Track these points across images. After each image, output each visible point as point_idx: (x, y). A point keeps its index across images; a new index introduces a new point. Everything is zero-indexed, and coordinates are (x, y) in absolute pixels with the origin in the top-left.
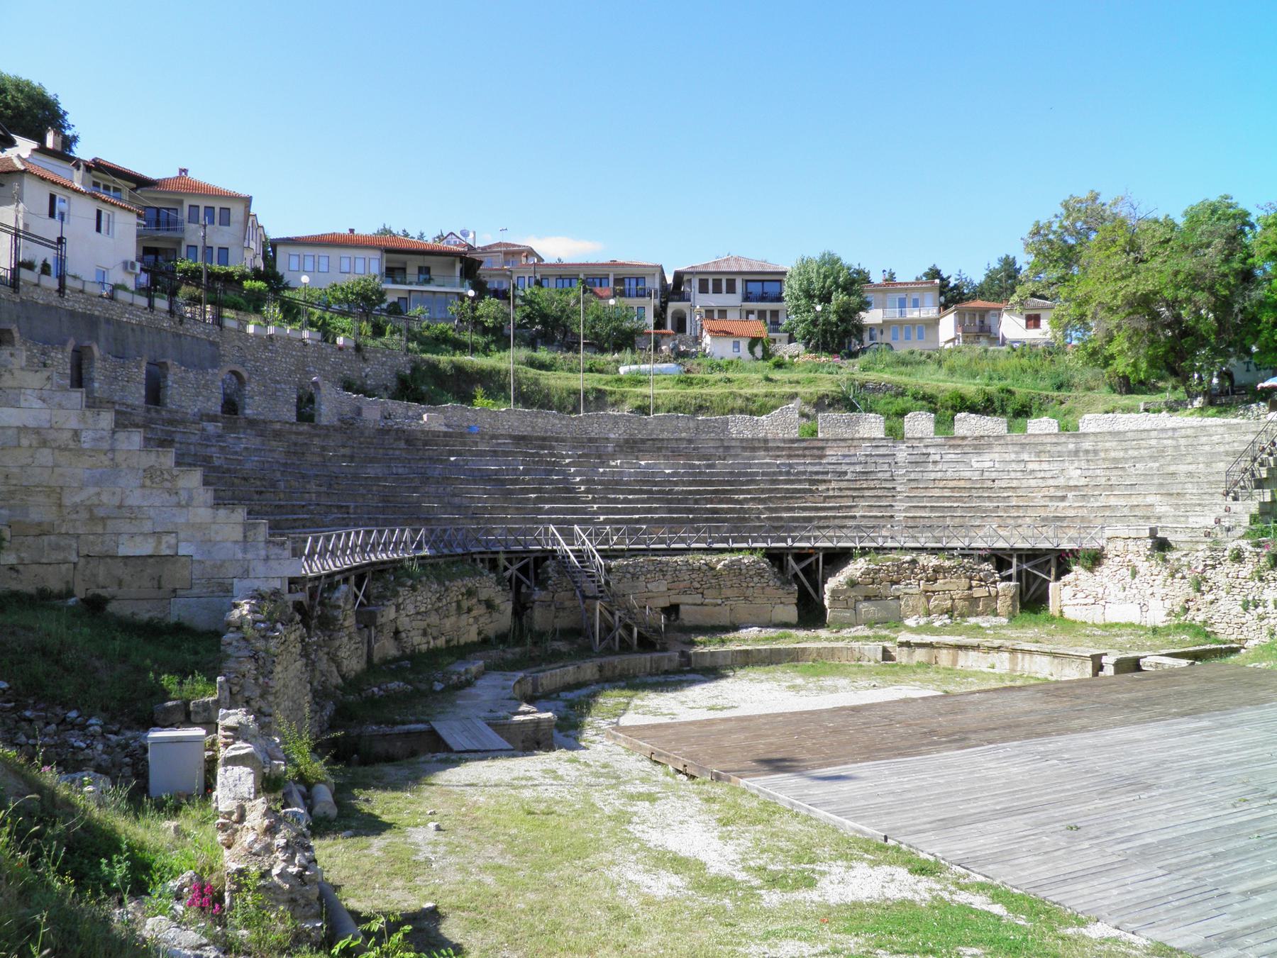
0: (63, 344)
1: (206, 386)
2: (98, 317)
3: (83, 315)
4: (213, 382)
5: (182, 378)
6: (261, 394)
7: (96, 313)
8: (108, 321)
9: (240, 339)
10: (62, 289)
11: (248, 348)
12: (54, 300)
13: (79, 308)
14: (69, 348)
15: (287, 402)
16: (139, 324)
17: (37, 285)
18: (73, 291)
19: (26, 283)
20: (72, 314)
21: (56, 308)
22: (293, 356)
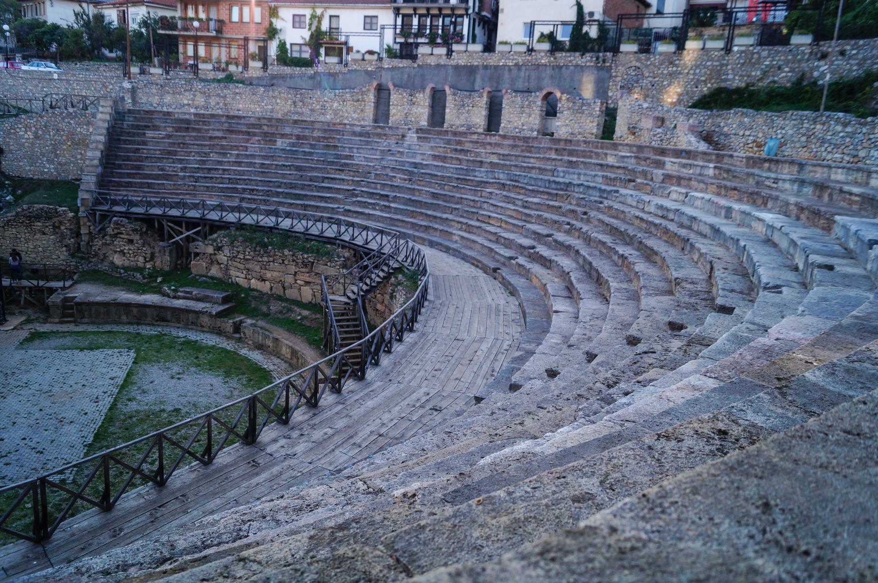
0: (423, 89)
1: (529, 106)
2: (477, 66)
3: (465, 67)
4: (535, 102)
5: (513, 101)
6: (569, 109)
7: (476, 64)
8: (486, 67)
9: (638, 60)
10: (450, 53)
11: (647, 66)
12: (443, 61)
13: (462, 62)
14: (428, 90)
15: (591, 115)
16: (516, 65)
17: (432, 54)
18: (459, 52)
19: (423, 55)
20: (457, 67)
21: (445, 66)
22: (705, 67)
